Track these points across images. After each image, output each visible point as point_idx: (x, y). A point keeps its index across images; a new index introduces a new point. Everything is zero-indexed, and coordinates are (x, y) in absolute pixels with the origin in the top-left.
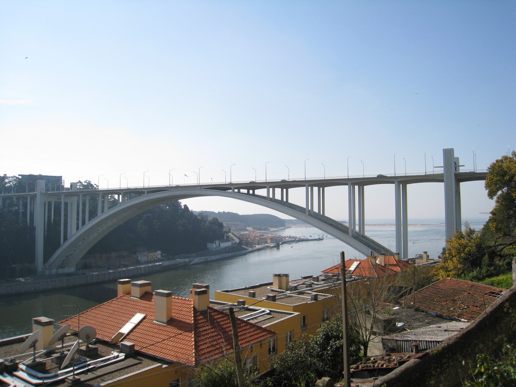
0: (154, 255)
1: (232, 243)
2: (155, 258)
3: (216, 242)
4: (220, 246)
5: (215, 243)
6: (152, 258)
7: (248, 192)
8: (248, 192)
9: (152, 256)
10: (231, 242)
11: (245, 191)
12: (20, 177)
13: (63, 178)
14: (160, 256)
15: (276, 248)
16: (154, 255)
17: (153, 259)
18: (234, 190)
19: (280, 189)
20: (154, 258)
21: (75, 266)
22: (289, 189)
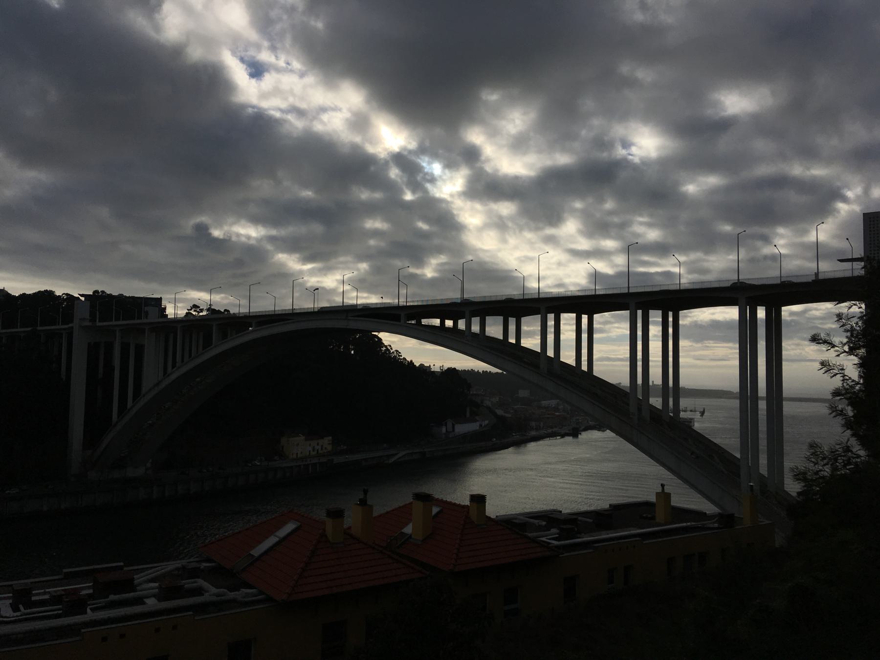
0: (318, 444)
1: (481, 425)
2: (319, 450)
3: (446, 423)
4: (454, 430)
5: (446, 425)
6: (313, 451)
7: (442, 323)
8: (442, 323)
9: (314, 447)
10: (478, 424)
11: (437, 322)
12: (83, 299)
13: (164, 303)
14: (330, 448)
15: (571, 438)
16: (318, 444)
17: (316, 452)
18: (405, 322)
19: (502, 318)
20: (318, 450)
21: (149, 465)
22: (524, 319)
